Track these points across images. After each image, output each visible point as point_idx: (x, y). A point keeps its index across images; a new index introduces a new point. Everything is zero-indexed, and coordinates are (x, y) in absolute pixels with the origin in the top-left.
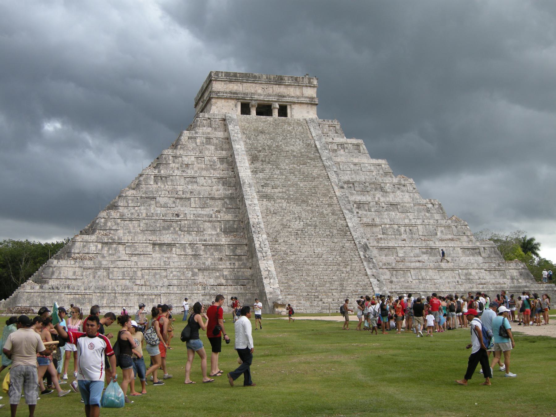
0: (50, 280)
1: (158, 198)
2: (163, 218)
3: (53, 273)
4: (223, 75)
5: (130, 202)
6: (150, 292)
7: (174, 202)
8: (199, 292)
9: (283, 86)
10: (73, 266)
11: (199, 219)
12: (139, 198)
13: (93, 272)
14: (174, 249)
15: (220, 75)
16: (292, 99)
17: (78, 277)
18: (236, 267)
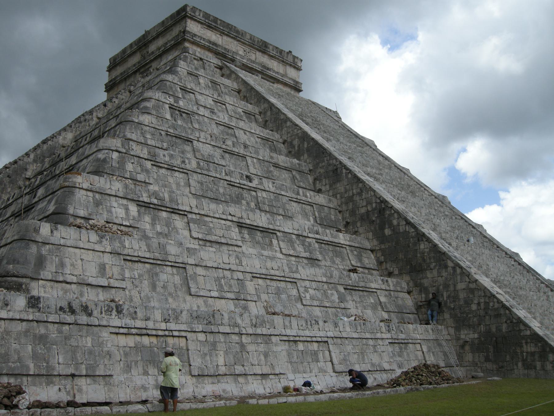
0: (34, 284)
1: (195, 143)
2: (228, 178)
3: (40, 262)
4: (201, 15)
5: (148, 136)
6: (307, 333)
7: (223, 157)
8: (384, 336)
9: (266, 56)
10: (97, 247)
11: (283, 193)
12: (163, 133)
13: (149, 271)
14: (275, 242)
15: (197, 14)
16: (276, 75)
17: (114, 283)
18: (392, 288)
